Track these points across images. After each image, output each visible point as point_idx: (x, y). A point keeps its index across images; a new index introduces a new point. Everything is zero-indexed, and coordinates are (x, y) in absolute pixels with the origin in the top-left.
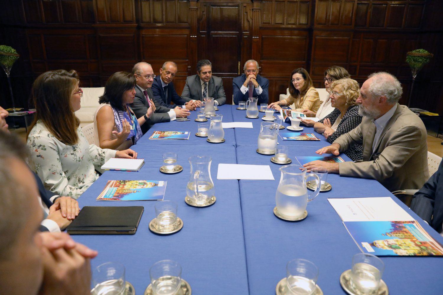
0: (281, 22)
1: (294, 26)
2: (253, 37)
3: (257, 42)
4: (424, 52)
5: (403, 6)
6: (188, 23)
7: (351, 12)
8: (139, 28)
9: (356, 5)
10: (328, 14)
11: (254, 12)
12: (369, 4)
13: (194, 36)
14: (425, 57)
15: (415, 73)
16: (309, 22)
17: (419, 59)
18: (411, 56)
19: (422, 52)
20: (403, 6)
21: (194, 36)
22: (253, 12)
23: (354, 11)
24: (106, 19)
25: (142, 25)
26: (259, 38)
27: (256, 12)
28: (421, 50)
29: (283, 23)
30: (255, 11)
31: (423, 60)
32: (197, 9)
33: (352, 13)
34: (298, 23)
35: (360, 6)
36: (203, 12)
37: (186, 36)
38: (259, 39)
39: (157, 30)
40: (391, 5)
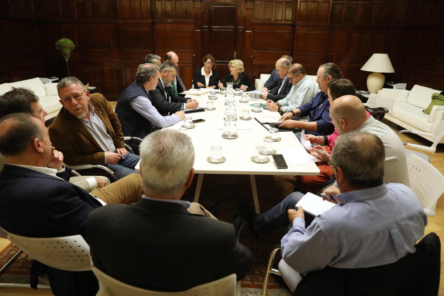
2: (247, 31)
9: (331, 4)
12: (343, 4)
13: (198, 30)
21: (198, 30)
23: (330, 9)
29: (271, 19)
32: (201, 7)
33: (328, 12)
36: (206, 10)
37: (192, 30)
39: (168, 25)
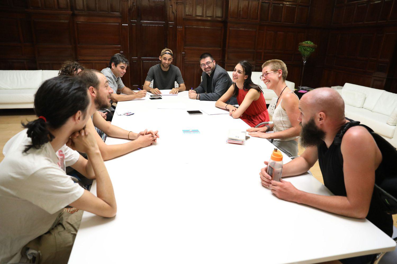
0: (201, 15)
1: (209, 18)
3: (181, 31)
4: (311, 43)
5: (295, 6)
6: (120, 13)
7: (257, 10)
8: (74, 15)
9: (260, 3)
10: (239, 10)
11: (178, 5)
12: (270, 3)
13: (125, 25)
14: (311, 47)
15: (305, 59)
16: (224, 16)
17: (307, 49)
18: (302, 46)
19: (309, 43)
20: (295, 6)
21: (125, 25)
22: (177, 5)
23: (259, 8)
24: (40, 5)
25: (76, 12)
26: (183, 28)
27: (179, 5)
28: (309, 42)
30: (179, 5)
31: (310, 49)
34: (214, 17)
35: (264, 4)
37: (118, 24)
38: (183, 29)
40: (287, 5)
